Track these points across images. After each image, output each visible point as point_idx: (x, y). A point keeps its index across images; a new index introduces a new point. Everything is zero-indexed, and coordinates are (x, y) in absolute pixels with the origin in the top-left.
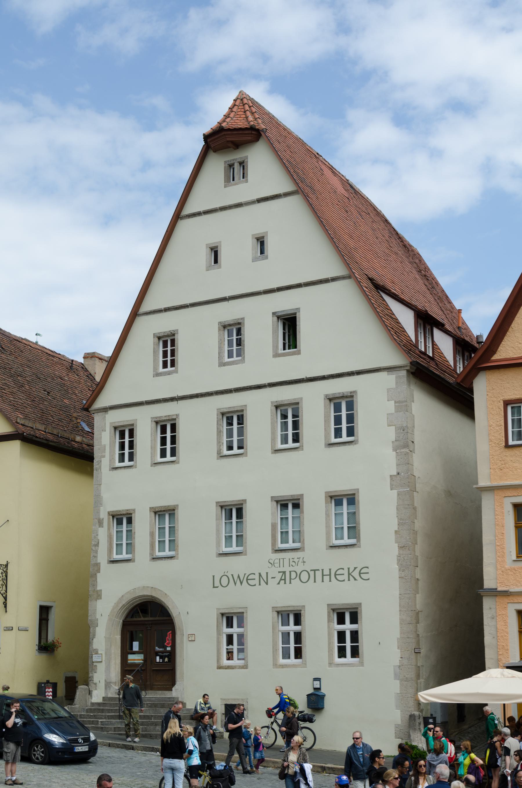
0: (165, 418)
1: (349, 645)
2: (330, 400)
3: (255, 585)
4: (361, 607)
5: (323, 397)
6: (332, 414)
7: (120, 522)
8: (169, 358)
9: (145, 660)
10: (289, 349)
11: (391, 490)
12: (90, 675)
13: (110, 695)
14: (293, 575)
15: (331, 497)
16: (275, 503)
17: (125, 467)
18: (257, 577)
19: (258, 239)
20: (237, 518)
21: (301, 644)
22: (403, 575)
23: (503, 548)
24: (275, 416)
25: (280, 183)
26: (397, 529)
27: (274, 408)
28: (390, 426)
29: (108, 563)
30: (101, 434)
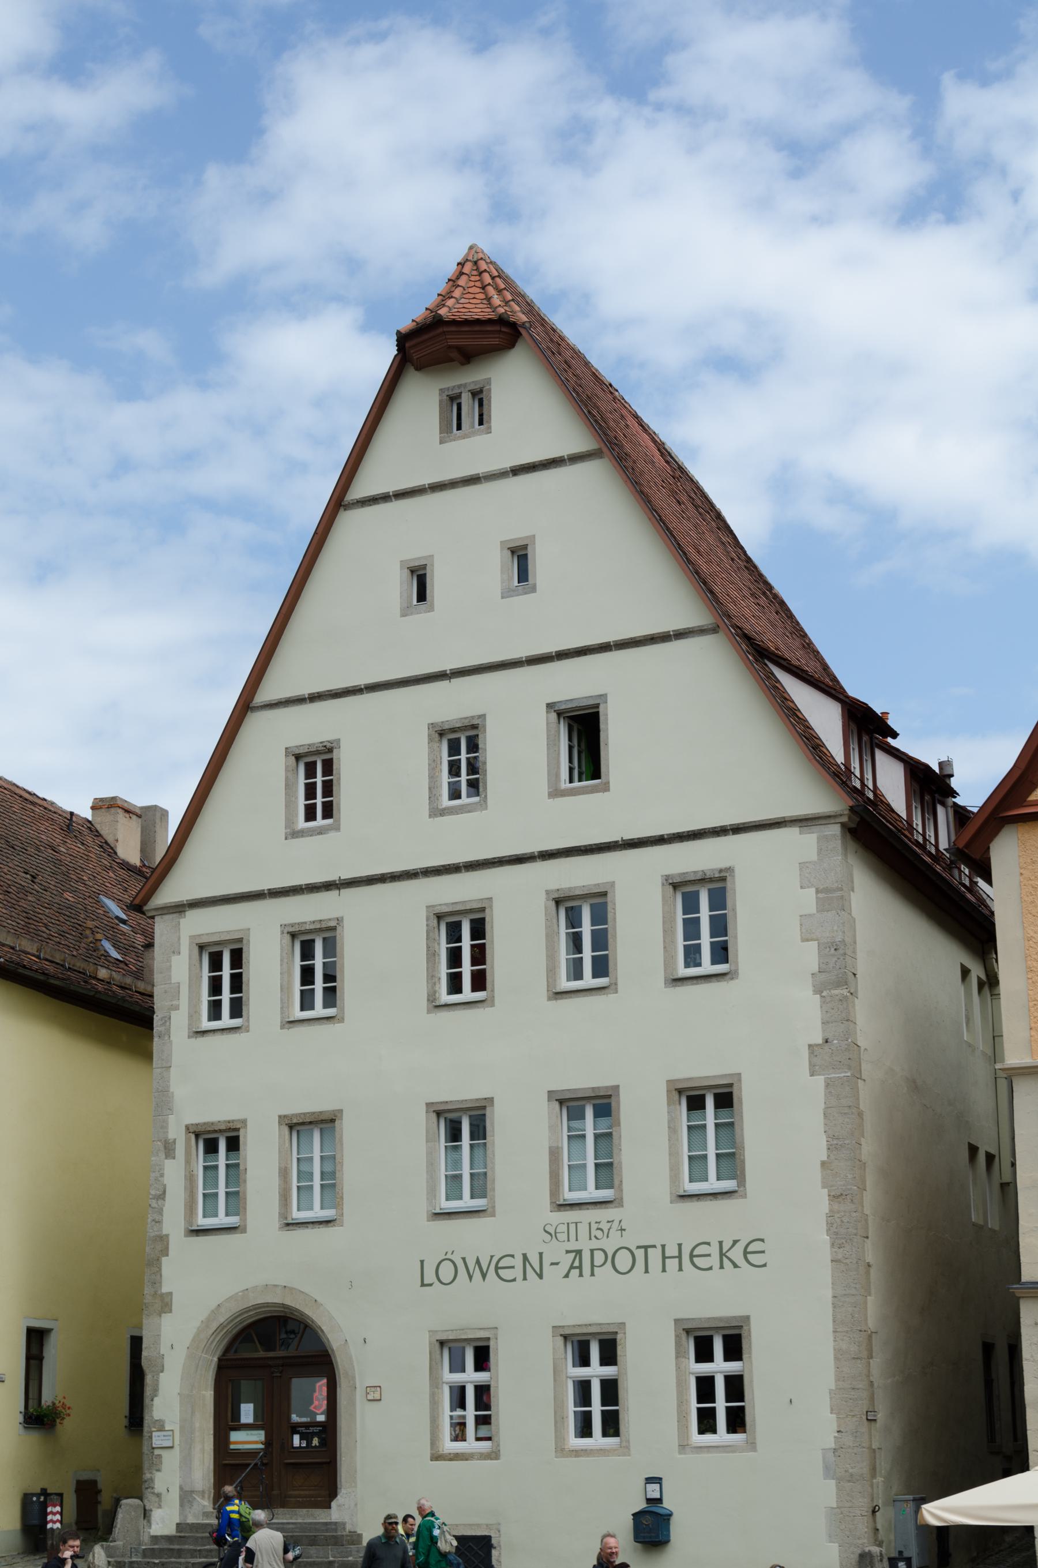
0: (312, 927)
1: (723, 1407)
2: (675, 886)
4: (749, 1325)
5: (659, 881)
6: (680, 917)
7: (211, 1147)
8: (319, 800)
9: (268, 1443)
10: (580, 780)
11: (812, 1075)
12: (147, 1476)
13: (191, 1520)
14: (599, 1258)
15: (680, 1092)
16: (557, 1105)
18: (518, 1262)
19: (513, 551)
21: (617, 1405)
22: (840, 1256)
24: (555, 921)
25: (564, 433)
26: (825, 1158)
27: (553, 903)
28: (807, 940)
29: (186, 1236)
30: (169, 961)
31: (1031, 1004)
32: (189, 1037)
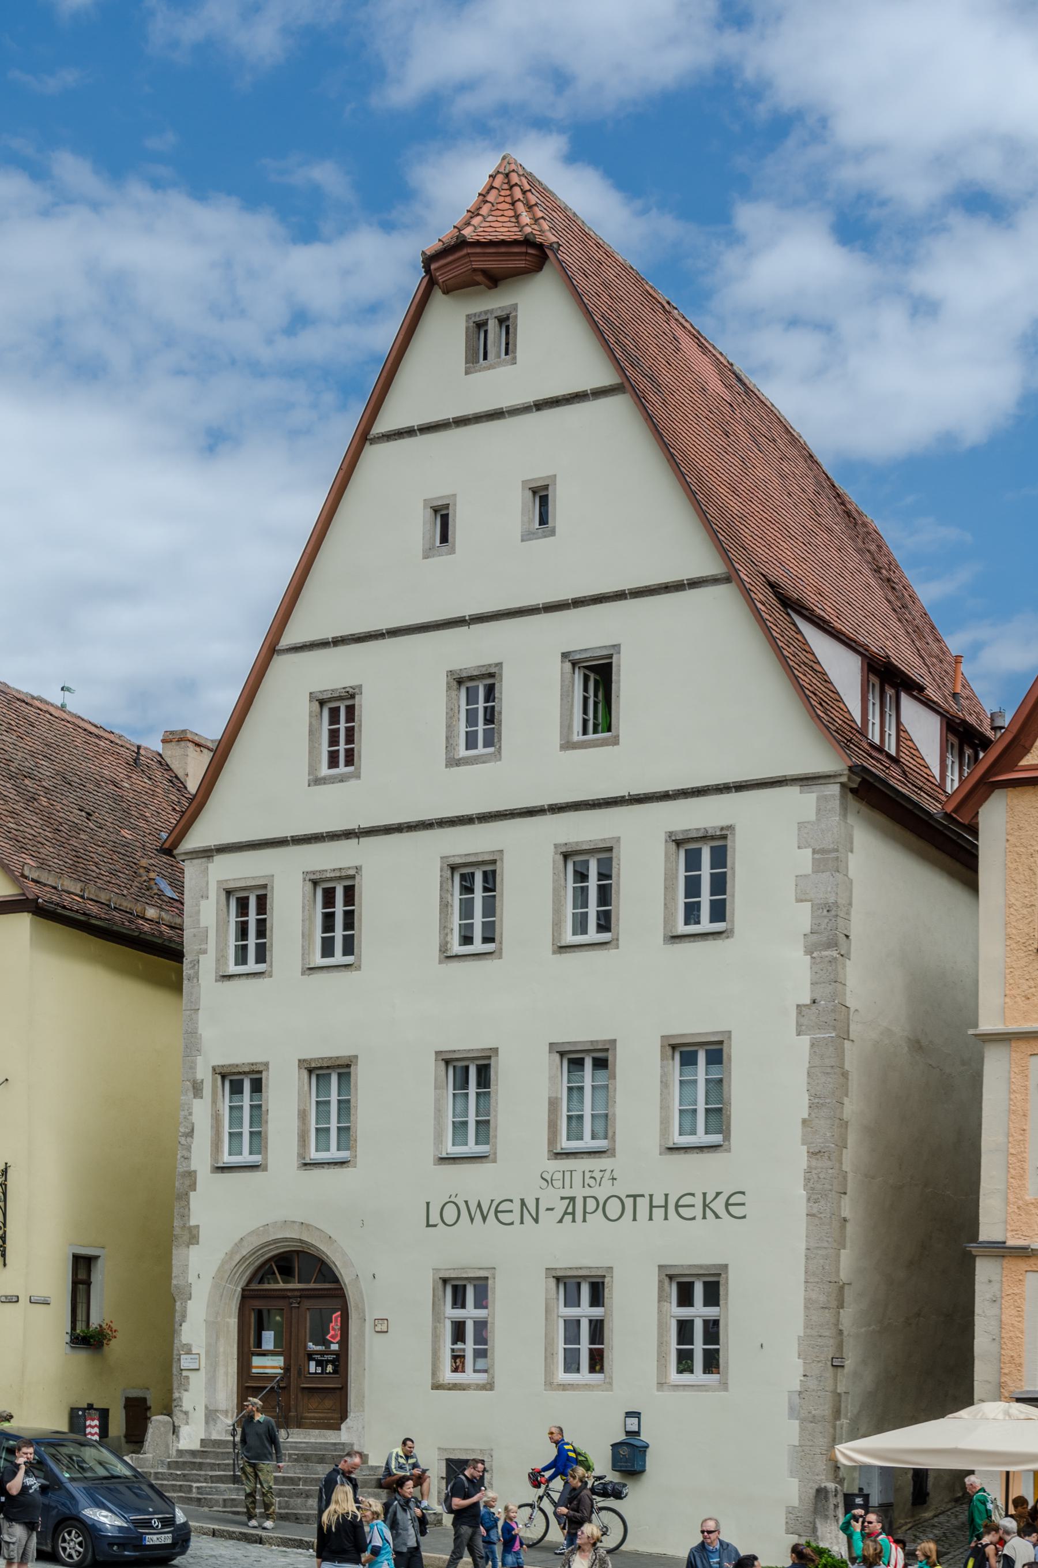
2: (678, 843)
3: (512, 1223)
4: (727, 1273)
6: (682, 874)
7: (236, 1089)
8: (342, 747)
10: (595, 731)
14: (591, 1205)
15: (674, 1047)
16: (557, 1057)
17: (248, 974)
18: (516, 1206)
20: (479, 1085)
22: (815, 1211)
23: (1023, 1161)
24: (562, 875)
26: (806, 1116)
27: (561, 857)
29: (212, 1172)
31: (1008, 971)
32: (216, 981)
